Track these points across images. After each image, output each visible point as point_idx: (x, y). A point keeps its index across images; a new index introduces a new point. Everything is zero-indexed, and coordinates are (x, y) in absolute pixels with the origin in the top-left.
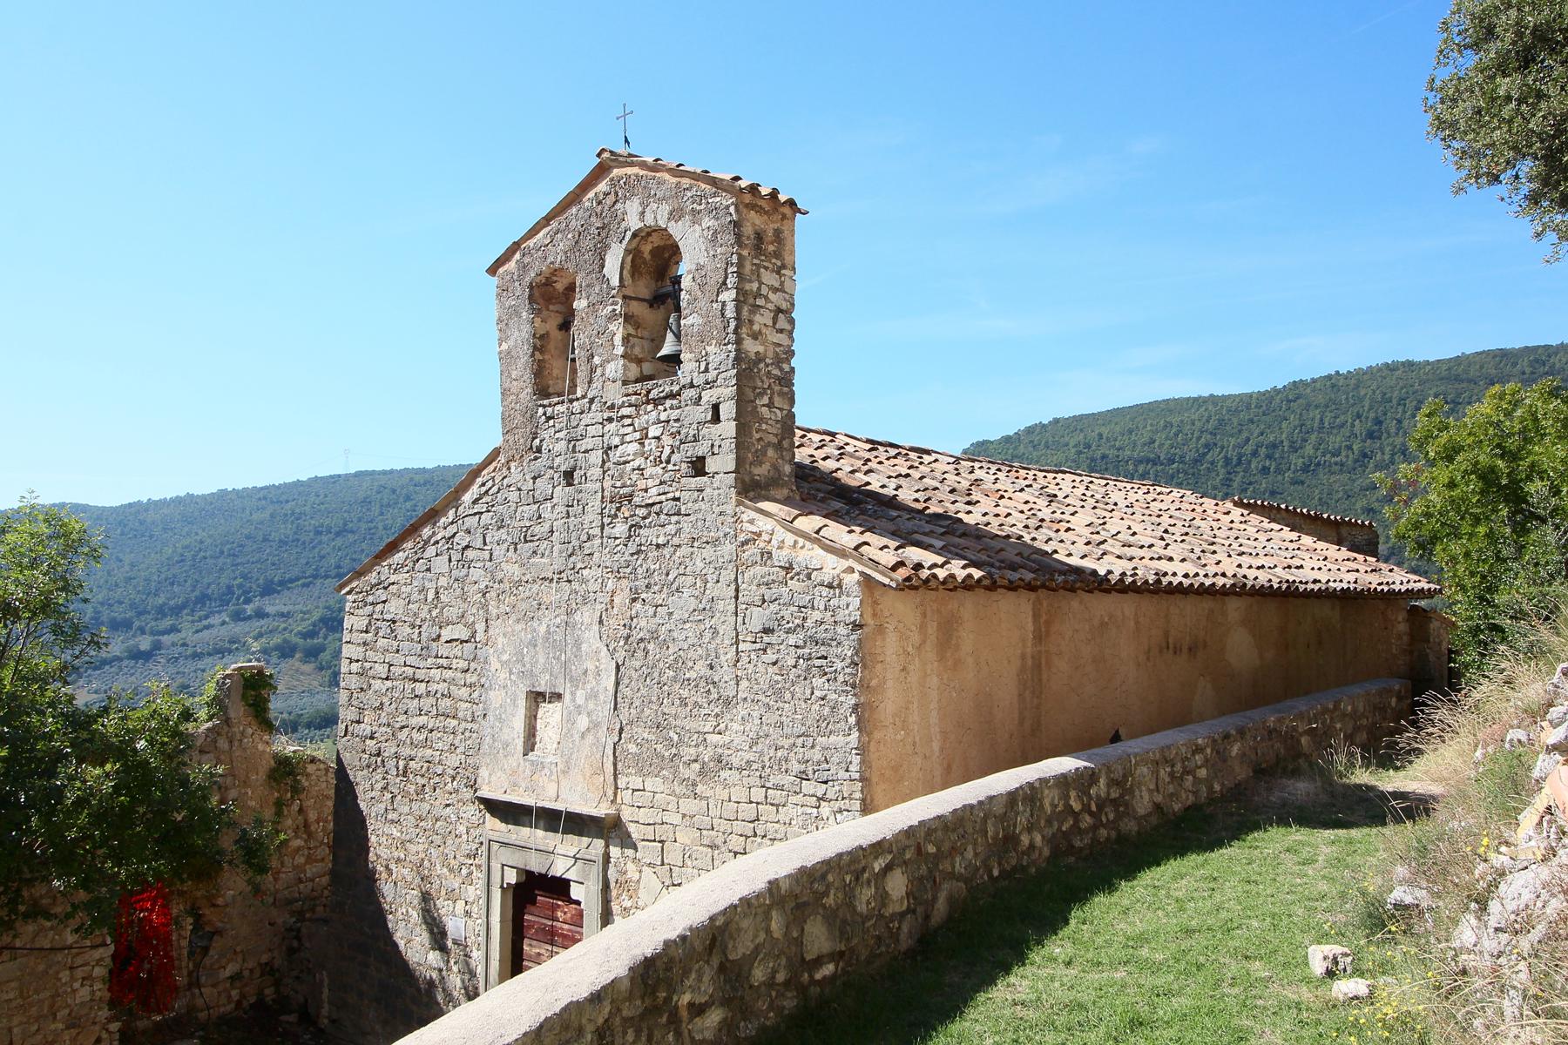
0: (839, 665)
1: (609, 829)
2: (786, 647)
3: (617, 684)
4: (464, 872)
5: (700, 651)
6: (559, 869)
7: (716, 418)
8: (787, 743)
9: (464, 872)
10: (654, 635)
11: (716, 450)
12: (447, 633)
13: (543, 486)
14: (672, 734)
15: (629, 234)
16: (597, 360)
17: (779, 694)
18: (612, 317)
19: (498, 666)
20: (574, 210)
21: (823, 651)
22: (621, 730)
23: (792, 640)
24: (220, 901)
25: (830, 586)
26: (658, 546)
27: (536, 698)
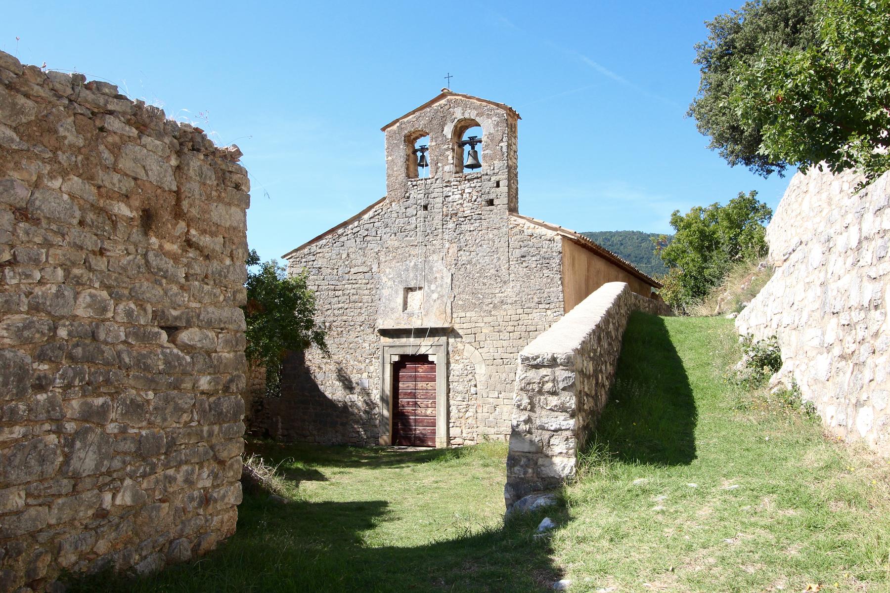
2: (532, 262)
4: (367, 361)
6: (422, 351)
7: (498, 186)
8: (532, 293)
9: (367, 361)
10: (470, 262)
12: (353, 270)
16: (439, 165)
17: (528, 277)
20: (428, 109)
21: (547, 261)
23: (534, 259)
27: (409, 290)
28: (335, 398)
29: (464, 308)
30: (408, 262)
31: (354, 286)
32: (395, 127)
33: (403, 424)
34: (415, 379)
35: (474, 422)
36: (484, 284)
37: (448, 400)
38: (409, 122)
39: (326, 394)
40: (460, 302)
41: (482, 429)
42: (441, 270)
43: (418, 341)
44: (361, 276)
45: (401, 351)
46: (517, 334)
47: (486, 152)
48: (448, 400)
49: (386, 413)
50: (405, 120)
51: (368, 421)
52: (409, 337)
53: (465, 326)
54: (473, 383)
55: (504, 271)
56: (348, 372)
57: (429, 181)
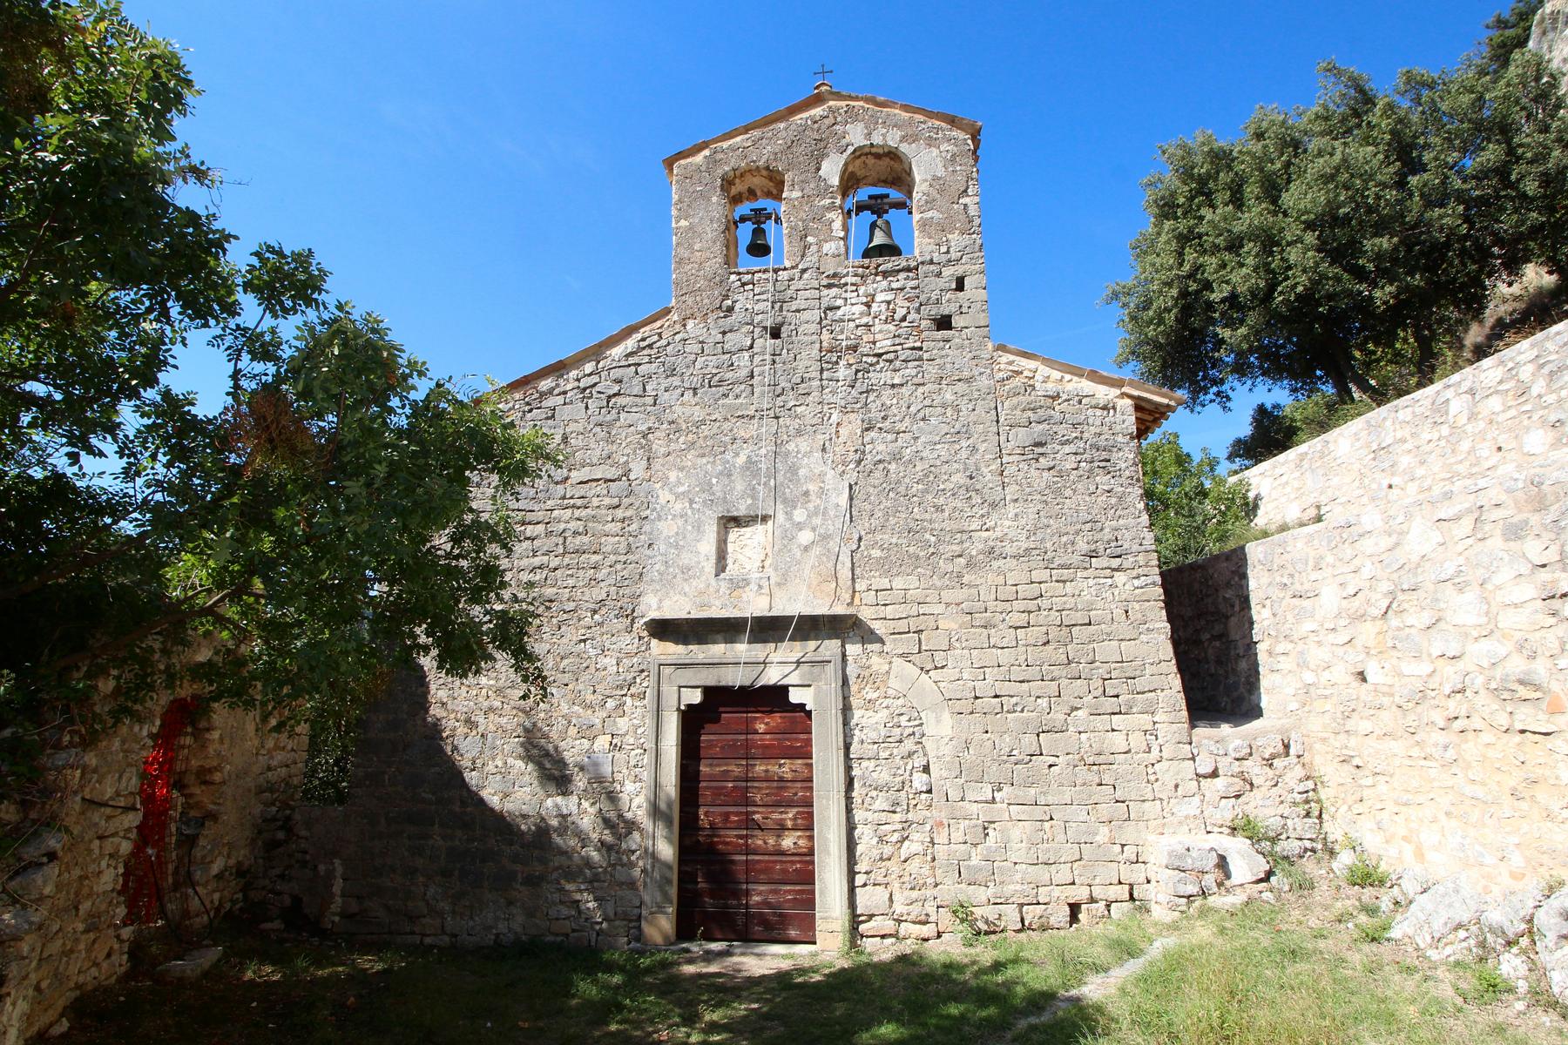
0: (1124, 466)
3: (851, 499)
4: (611, 704)
5: (956, 466)
6: (772, 677)
7: (960, 286)
9: (611, 704)
10: (896, 457)
12: (576, 476)
13: (739, 339)
14: (927, 536)
15: (851, 149)
16: (810, 239)
17: (1058, 492)
18: (832, 207)
20: (782, 125)
22: (860, 539)
23: (1067, 449)
24: (217, 777)
25: (1105, 408)
26: (893, 386)
27: (731, 521)
28: (509, 806)
30: (729, 456)
31: (577, 513)
32: (699, 158)
33: (710, 877)
34: (747, 753)
35: (926, 871)
36: (939, 509)
37: (849, 810)
38: (734, 149)
39: (484, 794)
40: (876, 553)
41: (951, 890)
42: (823, 477)
43: (759, 651)
44: (601, 488)
45: (711, 678)
46: (1035, 633)
47: (929, 214)
48: (849, 810)
49: (666, 850)
50: (725, 145)
51: (613, 871)
52: (731, 640)
54: (919, 761)
55: (988, 475)
56: (554, 735)
57: (783, 275)
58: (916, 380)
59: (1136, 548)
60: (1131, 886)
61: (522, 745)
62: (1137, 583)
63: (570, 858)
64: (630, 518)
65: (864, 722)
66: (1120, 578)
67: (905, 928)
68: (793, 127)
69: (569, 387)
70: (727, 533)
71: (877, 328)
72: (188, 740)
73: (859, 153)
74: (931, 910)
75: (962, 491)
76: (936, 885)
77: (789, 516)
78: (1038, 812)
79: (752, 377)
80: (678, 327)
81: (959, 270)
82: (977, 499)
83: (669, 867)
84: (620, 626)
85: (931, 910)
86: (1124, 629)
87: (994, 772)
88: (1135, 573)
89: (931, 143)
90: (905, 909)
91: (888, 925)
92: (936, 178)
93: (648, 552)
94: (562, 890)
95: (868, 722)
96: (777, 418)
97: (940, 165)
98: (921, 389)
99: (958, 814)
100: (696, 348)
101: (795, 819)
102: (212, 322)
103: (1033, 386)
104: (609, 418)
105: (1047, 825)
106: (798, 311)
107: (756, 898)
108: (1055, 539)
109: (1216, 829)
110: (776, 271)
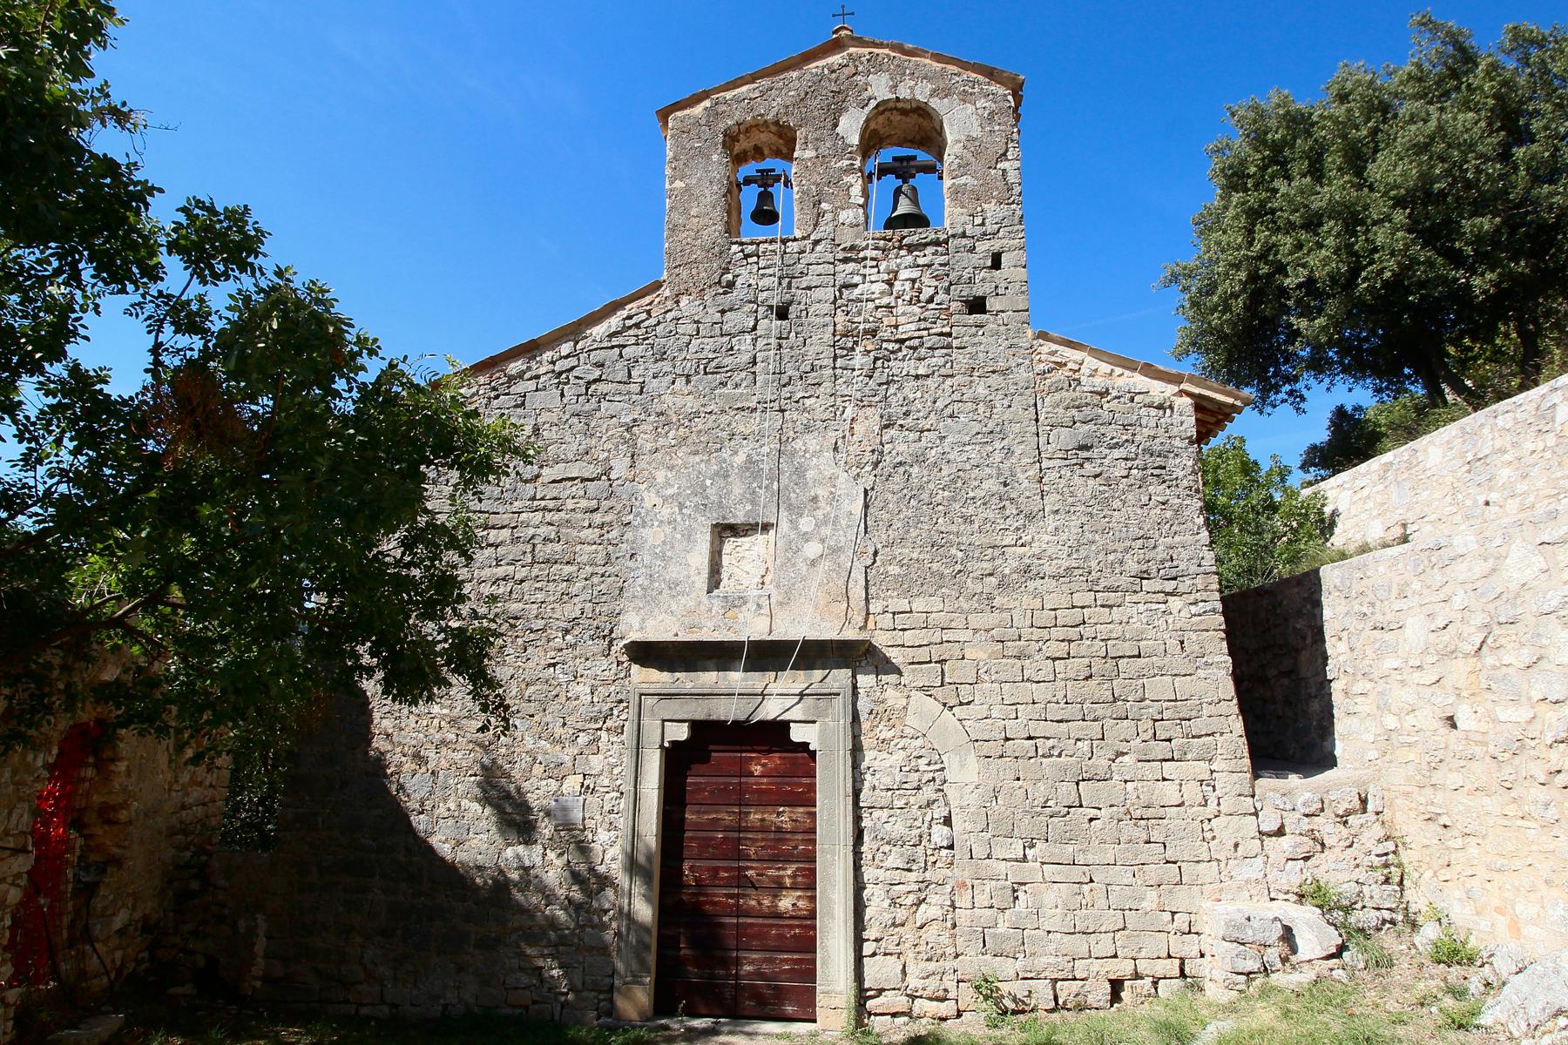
1: (855, 655)
3: (866, 506)
4: (583, 739)
5: (988, 470)
6: (771, 710)
7: (996, 263)
8: (1120, 546)
9: (583, 739)
10: (919, 459)
11: (1001, 291)
12: (548, 473)
14: (954, 551)
15: (873, 104)
18: (850, 170)
19: (659, 501)
20: (795, 74)
21: (1159, 461)
22: (876, 553)
23: (1117, 453)
24: (123, 815)
25: (1160, 407)
26: (917, 377)
27: (726, 531)
28: (462, 856)
29: (905, 586)
30: (725, 454)
31: (549, 517)
32: (698, 110)
34: (740, 798)
35: (945, 939)
36: (968, 520)
37: (857, 867)
39: (434, 841)
40: (894, 570)
41: (974, 963)
43: (757, 681)
44: (576, 490)
45: (699, 711)
46: (1076, 666)
48: (857, 867)
49: (644, 911)
50: (729, 95)
53: (900, 637)
54: (939, 812)
55: (1025, 482)
56: (516, 774)
58: (943, 371)
59: (1193, 569)
60: (1182, 960)
61: (479, 784)
62: (1194, 609)
63: (532, 917)
64: (610, 524)
65: (876, 763)
66: (1175, 603)
67: (920, 1006)
68: (808, 76)
69: (542, 370)
70: (722, 543)
71: (900, 310)
72: (90, 772)
73: (883, 108)
74: (951, 986)
75: (995, 500)
76: (957, 956)
77: (794, 524)
78: (1076, 873)
79: (755, 363)
80: (669, 304)
81: (996, 245)
82: (1011, 510)
83: (647, 929)
84: (595, 649)
85: (951, 986)
86: (1178, 663)
87: (1026, 826)
88: (1192, 598)
89: (966, 97)
90: (919, 984)
91: (901, 1003)
92: (970, 139)
93: (631, 564)
94: (523, 954)
95: (882, 765)
96: (782, 411)
97: (976, 124)
98: (949, 382)
99: (983, 874)
100: (691, 328)
101: (794, 876)
102: (130, 287)
103: (1078, 380)
104: (587, 407)
105: (1086, 888)
106: (809, 288)
107: (748, 968)
108: (1101, 557)
109: (1281, 896)
110: (784, 242)
